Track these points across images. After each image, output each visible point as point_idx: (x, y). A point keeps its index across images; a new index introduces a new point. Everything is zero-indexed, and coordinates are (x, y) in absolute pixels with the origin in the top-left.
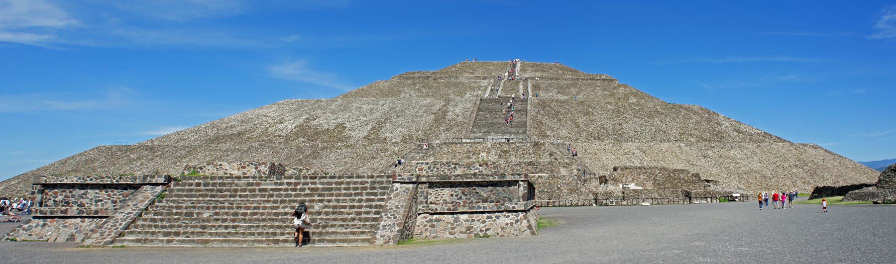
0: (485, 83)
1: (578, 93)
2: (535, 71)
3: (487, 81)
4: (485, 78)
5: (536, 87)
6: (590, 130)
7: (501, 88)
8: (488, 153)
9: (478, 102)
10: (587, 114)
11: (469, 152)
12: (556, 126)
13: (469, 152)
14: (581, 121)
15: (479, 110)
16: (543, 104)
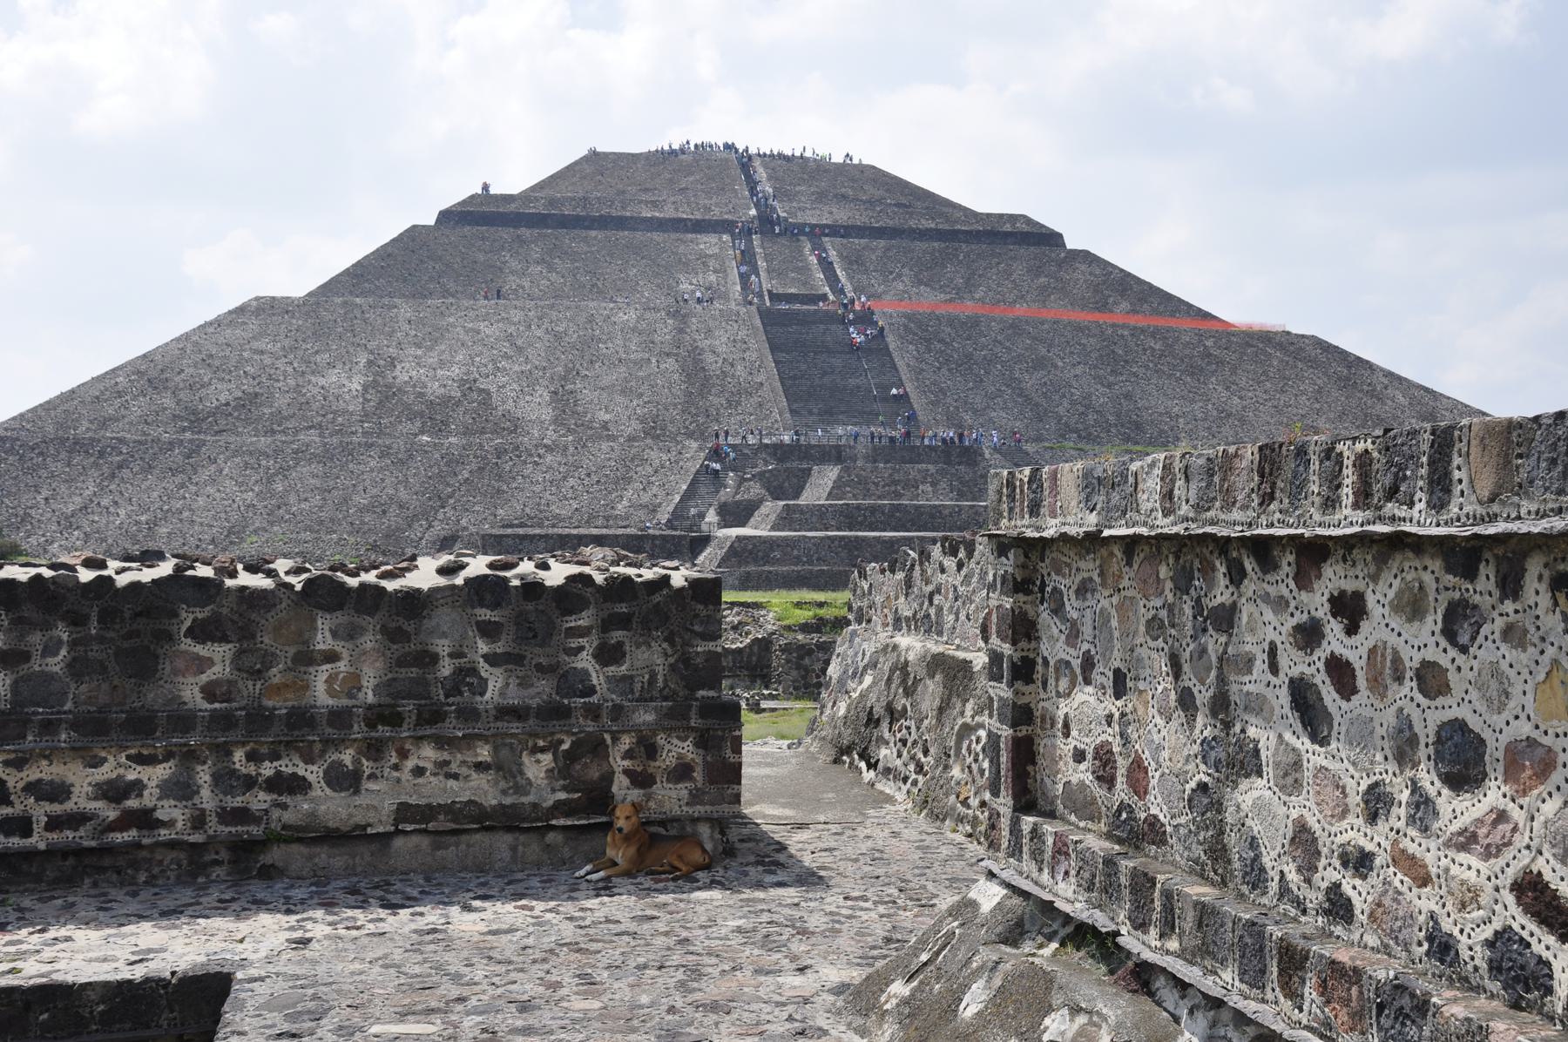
0: (709, 243)
1: (970, 286)
2: (821, 197)
3: (712, 238)
4: (700, 227)
5: (854, 262)
6: (1061, 410)
7: (762, 264)
8: (933, 484)
9: (758, 322)
10: (1040, 364)
11: (895, 482)
12: (978, 401)
13: (895, 482)
14: (1030, 382)
15: (774, 349)
16: (920, 330)
